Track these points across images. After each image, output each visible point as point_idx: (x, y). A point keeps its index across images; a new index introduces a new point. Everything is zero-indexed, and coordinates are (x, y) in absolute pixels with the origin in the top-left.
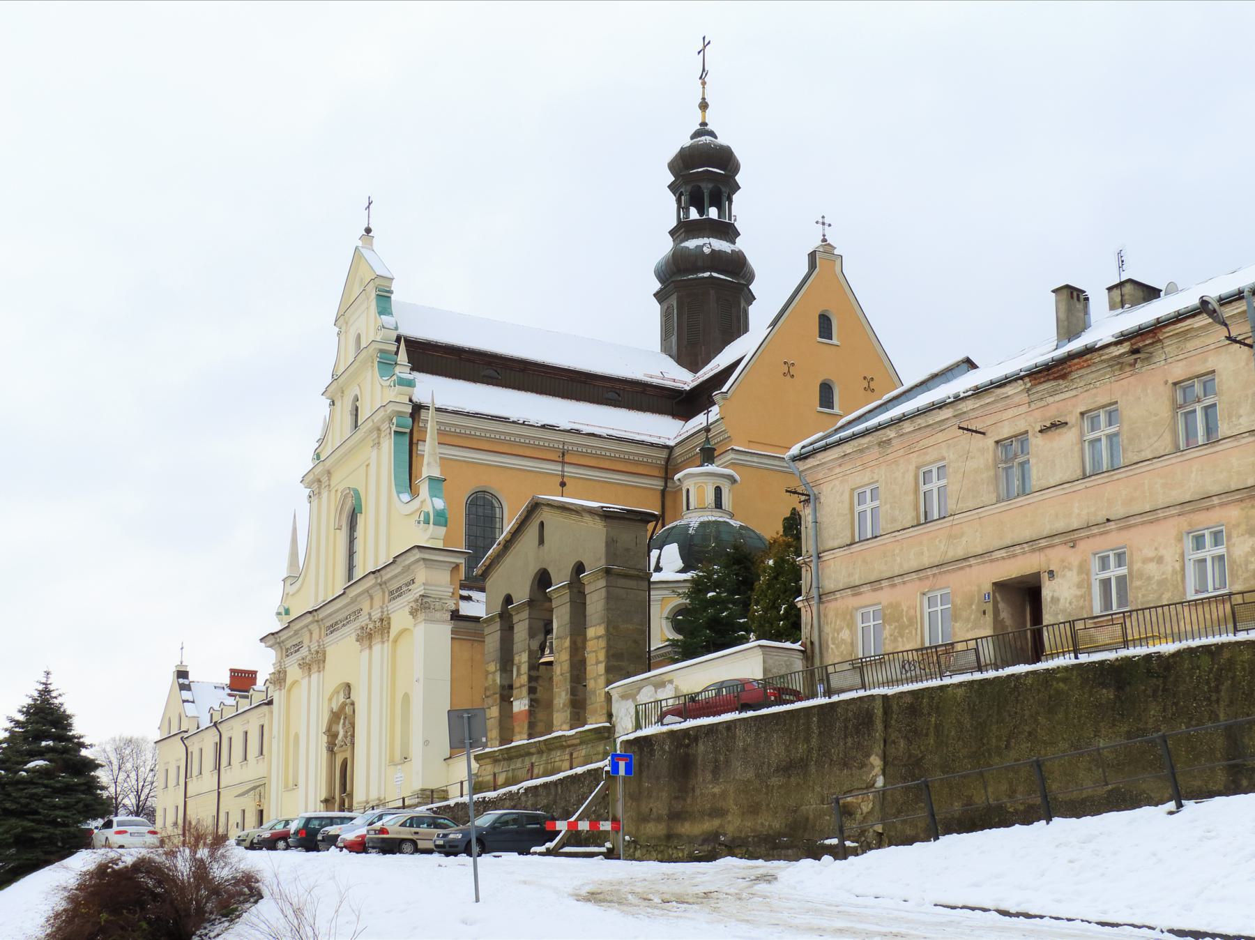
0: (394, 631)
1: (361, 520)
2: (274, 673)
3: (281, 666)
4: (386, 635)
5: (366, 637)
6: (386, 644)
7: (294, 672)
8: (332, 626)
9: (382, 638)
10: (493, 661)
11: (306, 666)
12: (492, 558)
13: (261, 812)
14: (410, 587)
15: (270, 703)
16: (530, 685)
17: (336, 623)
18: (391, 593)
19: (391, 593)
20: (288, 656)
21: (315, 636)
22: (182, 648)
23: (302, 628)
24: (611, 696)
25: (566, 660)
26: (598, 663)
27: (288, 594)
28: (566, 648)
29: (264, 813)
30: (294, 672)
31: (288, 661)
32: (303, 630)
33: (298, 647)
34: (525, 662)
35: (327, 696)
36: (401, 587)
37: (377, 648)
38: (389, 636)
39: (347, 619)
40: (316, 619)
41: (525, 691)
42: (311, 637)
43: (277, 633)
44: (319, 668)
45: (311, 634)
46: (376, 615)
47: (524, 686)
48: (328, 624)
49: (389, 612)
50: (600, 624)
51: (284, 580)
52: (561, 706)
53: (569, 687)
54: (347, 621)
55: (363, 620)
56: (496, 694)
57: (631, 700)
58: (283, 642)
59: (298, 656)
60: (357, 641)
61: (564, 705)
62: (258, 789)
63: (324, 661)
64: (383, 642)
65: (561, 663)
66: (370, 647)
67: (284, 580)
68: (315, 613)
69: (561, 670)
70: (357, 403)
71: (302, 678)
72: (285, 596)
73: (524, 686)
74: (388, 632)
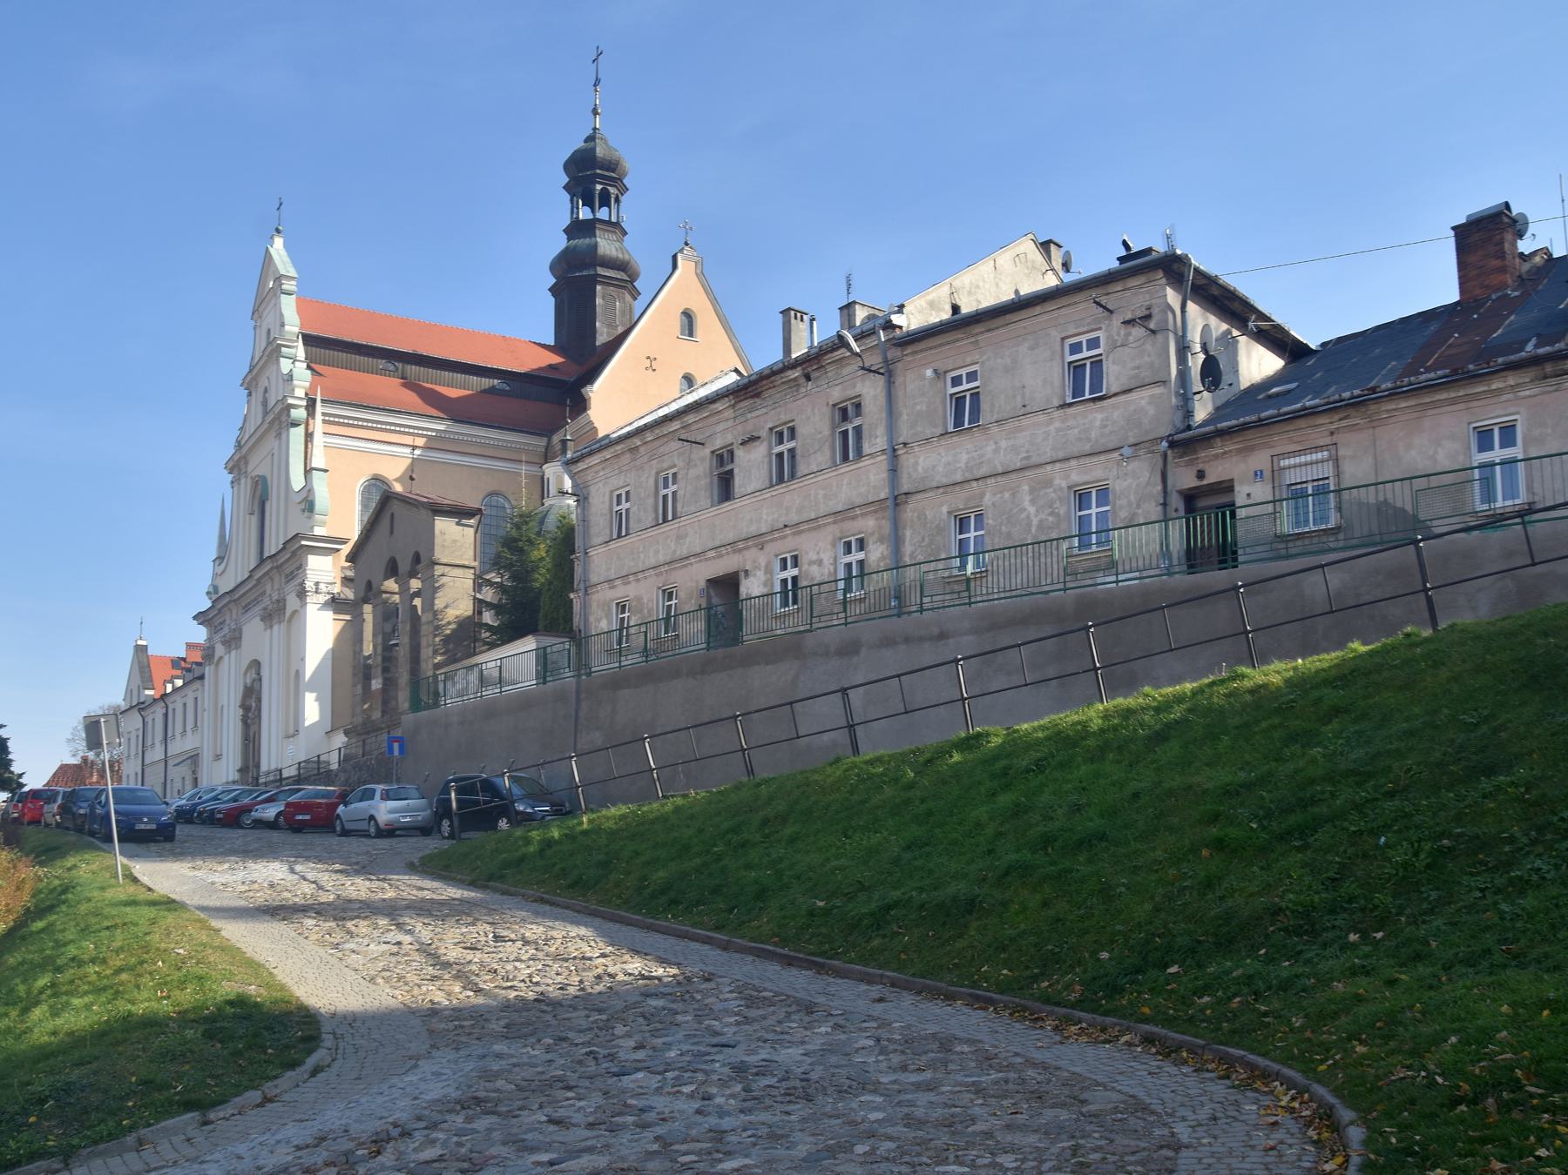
17: (249, 603)
18: (287, 576)
19: (287, 576)
35: (242, 672)
48: (244, 604)
63: (240, 638)
66: (271, 627)
72: (215, 575)
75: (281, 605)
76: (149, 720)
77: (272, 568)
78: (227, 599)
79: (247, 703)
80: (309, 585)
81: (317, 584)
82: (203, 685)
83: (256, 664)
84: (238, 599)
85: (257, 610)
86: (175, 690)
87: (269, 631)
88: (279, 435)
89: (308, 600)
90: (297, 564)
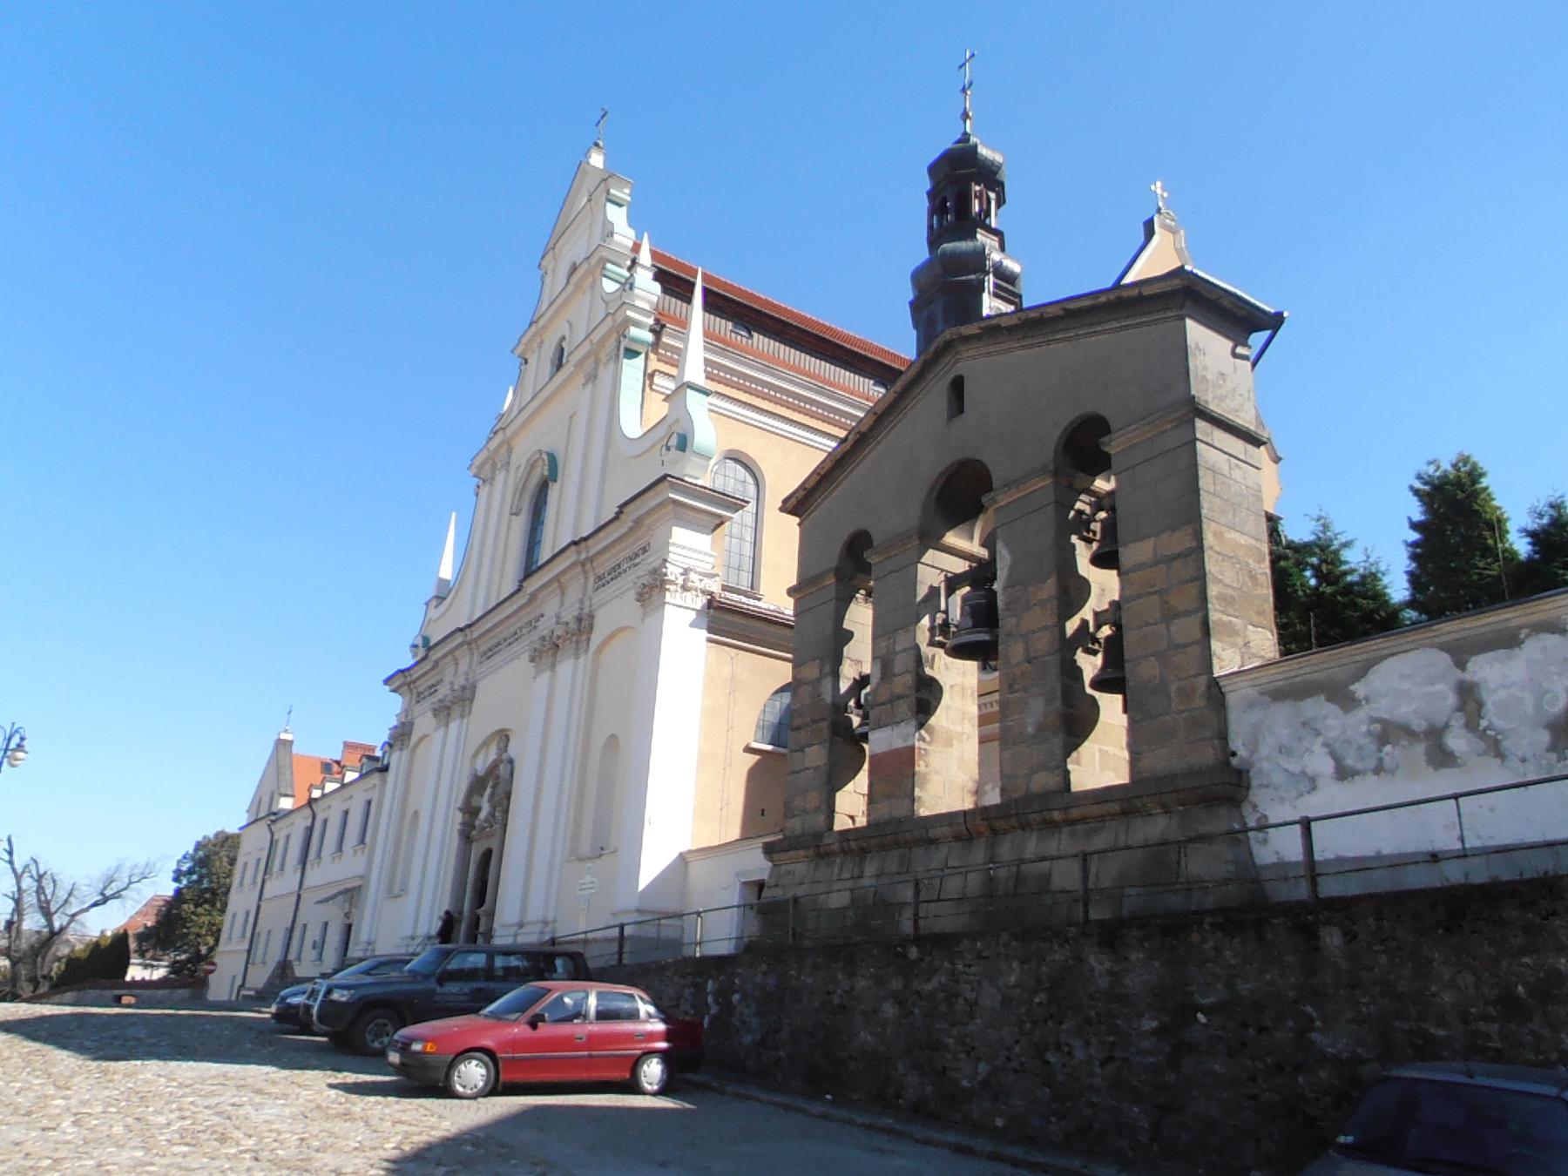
0: (597, 638)
1: (553, 492)
2: (396, 727)
3: (407, 716)
4: (585, 643)
5: (548, 651)
6: (582, 660)
7: (425, 722)
8: (490, 650)
9: (577, 649)
10: (813, 660)
11: (444, 712)
12: (822, 473)
13: (349, 927)
14: (637, 561)
15: (385, 769)
16: (919, 695)
17: (499, 644)
19: (600, 578)
20: (418, 702)
21: (463, 666)
22: (290, 712)
23: (444, 656)
24: (1223, 694)
25: (1045, 628)
26: (1170, 616)
27: (430, 620)
28: (1041, 603)
29: (353, 928)
30: (425, 722)
31: (418, 709)
32: (446, 660)
33: (433, 689)
34: (905, 650)
35: (471, 750)
36: (619, 565)
37: (565, 667)
38: (588, 645)
39: (516, 634)
40: (468, 638)
41: (904, 708)
42: (456, 669)
43: (408, 669)
44: (463, 711)
45: (457, 664)
46: (569, 615)
47: (899, 697)
48: (484, 648)
49: (593, 607)
50: (1173, 529)
51: (427, 604)
52: (1030, 730)
53: (1058, 687)
54: (516, 636)
55: (544, 627)
56: (823, 719)
57: (1322, 697)
58: (414, 682)
59: (435, 699)
60: (532, 660)
61: (1040, 728)
62: (351, 894)
63: (472, 701)
64: (577, 657)
65: (1022, 636)
66: (553, 667)
67: (427, 604)
68: (467, 631)
69: (1027, 650)
70: (564, 344)
71: (436, 730)
72: (427, 622)
73: (899, 697)
74: (589, 639)
75: (584, 625)
76: (280, 836)
77: (573, 564)
78: (459, 638)
79: (474, 802)
80: (672, 572)
81: (686, 572)
82: (384, 782)
83: (503, 737)
84: (476, 640)
85: (523, 647)
86: (324, 795)
87: (546, 675)
88: (592, 378)
89: (668, 597)
90: (641, 544)
